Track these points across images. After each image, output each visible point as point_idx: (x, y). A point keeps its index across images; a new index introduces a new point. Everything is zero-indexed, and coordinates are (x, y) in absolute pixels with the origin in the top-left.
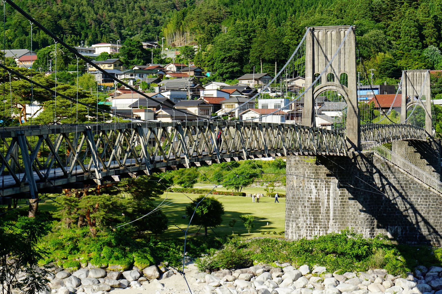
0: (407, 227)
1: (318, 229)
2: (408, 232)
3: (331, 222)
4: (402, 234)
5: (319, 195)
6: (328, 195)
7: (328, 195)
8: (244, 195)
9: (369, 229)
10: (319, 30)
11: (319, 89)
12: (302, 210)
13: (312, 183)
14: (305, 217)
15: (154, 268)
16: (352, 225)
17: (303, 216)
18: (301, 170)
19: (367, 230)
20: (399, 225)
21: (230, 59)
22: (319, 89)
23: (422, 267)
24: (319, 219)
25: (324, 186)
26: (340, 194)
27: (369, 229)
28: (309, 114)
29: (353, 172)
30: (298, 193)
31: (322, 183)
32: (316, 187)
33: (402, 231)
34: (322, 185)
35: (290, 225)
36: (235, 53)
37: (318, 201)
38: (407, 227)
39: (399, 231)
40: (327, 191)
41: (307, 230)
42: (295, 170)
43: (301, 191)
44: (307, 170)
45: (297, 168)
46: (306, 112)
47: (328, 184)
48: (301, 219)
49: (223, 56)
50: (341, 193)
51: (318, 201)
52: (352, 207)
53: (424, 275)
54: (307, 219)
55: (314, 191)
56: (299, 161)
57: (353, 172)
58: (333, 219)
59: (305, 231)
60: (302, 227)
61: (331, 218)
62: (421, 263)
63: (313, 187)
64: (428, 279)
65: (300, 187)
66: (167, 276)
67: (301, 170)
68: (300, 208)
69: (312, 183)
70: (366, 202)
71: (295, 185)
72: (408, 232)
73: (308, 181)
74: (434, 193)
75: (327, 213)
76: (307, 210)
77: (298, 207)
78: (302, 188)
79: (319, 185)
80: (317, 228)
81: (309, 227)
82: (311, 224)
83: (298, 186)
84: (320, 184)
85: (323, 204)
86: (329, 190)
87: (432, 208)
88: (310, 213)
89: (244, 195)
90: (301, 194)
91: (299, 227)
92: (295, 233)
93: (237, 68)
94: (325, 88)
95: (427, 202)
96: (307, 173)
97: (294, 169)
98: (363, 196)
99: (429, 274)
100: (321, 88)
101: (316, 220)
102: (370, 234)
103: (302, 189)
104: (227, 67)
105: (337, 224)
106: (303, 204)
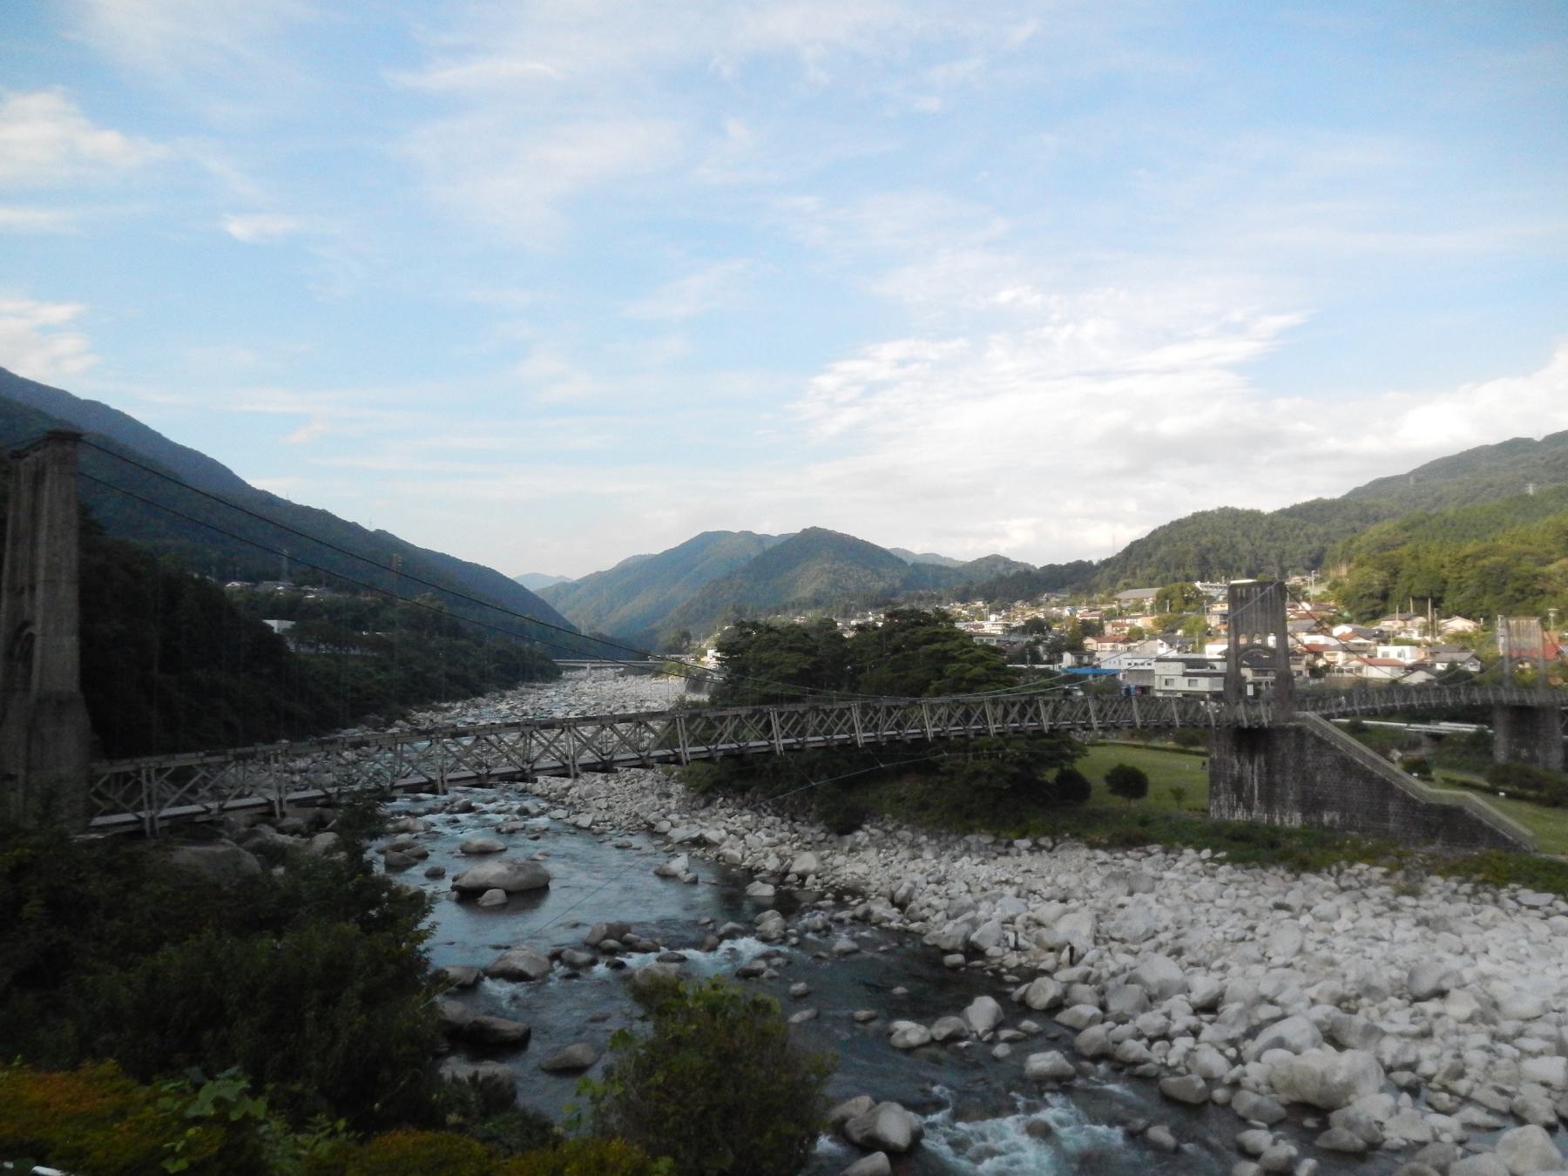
3: (1256, 803)
6: (1253, 772)
7: (1253, 772)
15: (1047, 838)
21: (1371, 596)
23: (1343, 863)
32: (1239, 761)
36: (1377, 587)
39: (1337, 818)
45: (1217, 740)
48: (1222, 797)
49: (1361, 593)
53: (1340, 872)
55: (1237, 766)
61: (1256, 797)
62: (1346, 858)
63: (1236, 762)
64: (1343, 877)
66: (1062, 849)
68: (1221, 785)
76: (1229, 788)
85: (1247, 779)
93: (1380, 607)
94: (1251, 650)
99: (1347, 871)
101: (1239, 799)
104: (1367, 605)
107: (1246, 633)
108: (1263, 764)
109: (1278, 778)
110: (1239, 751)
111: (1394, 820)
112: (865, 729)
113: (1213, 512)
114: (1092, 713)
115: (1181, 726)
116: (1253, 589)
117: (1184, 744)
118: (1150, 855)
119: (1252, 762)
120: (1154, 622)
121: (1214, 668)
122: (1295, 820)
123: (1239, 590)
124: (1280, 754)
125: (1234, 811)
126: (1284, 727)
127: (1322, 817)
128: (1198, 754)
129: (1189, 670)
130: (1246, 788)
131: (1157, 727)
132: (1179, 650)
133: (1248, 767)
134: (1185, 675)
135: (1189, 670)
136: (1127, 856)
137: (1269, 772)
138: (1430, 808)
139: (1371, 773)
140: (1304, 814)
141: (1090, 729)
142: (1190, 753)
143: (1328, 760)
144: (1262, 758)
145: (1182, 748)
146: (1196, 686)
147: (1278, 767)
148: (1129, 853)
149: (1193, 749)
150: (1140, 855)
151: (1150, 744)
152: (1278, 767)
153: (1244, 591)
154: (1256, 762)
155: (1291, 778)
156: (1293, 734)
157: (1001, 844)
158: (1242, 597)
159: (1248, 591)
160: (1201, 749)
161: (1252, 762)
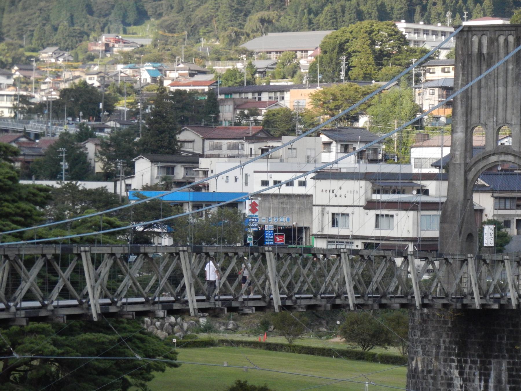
10: (482, 33)
11: (479, 161)
13: (454, 365)
18: (432, 336)
22: (479, 161)
25: (477, 373)
28: (454, 214)
30: (425, 386)
31: (474, 366)
32: (461, 374)
40: (482, 383)
42: (421, 335)
43: (431, 381)
44: (444, 336)
45: (424, 333)
46: (450, 209)
47: (486, 369)
55: (458, 382)
56: (428, 315)
63: (456, 373)
65: (429, 372)
67: (432, 336)
69: (454, 365)
71: (420, 369)
73: (445, 361)
78: (432, 374)
79: (467, 370)
83: (425, 369)
84: (470, 368)
86: (486, 381)
90: (431, 387)
94: (493, 159)
96: (444, 342)
97: (419, 333)
100: (484, 158)
103: (432, 378)
107: (485, 125)
108: (504, 377)
110: (462, 353)
114: (187, 280)
115: (357, 306)
116: (502, 39)
117: (365, 343)
119: (485, 376)
120: (315, 98)
121: (426, 192)
123: (475, 39)
128: (387, 360)
129: (377, 197)
131: (309, 307)
132: (360, 155)
133: (478, 383)
134: (370, 205)
135: (377, 197)
141: (183, 313)
142: (373, 359)
144: (504, 366)
145: (360, 349)
146: (390, 227)
149: (378, 350)
151: (298, 342)
153: (485, 41)
154: (493, 374)
159: (492, 42)
160: (394, 351)
161: (485, 376)
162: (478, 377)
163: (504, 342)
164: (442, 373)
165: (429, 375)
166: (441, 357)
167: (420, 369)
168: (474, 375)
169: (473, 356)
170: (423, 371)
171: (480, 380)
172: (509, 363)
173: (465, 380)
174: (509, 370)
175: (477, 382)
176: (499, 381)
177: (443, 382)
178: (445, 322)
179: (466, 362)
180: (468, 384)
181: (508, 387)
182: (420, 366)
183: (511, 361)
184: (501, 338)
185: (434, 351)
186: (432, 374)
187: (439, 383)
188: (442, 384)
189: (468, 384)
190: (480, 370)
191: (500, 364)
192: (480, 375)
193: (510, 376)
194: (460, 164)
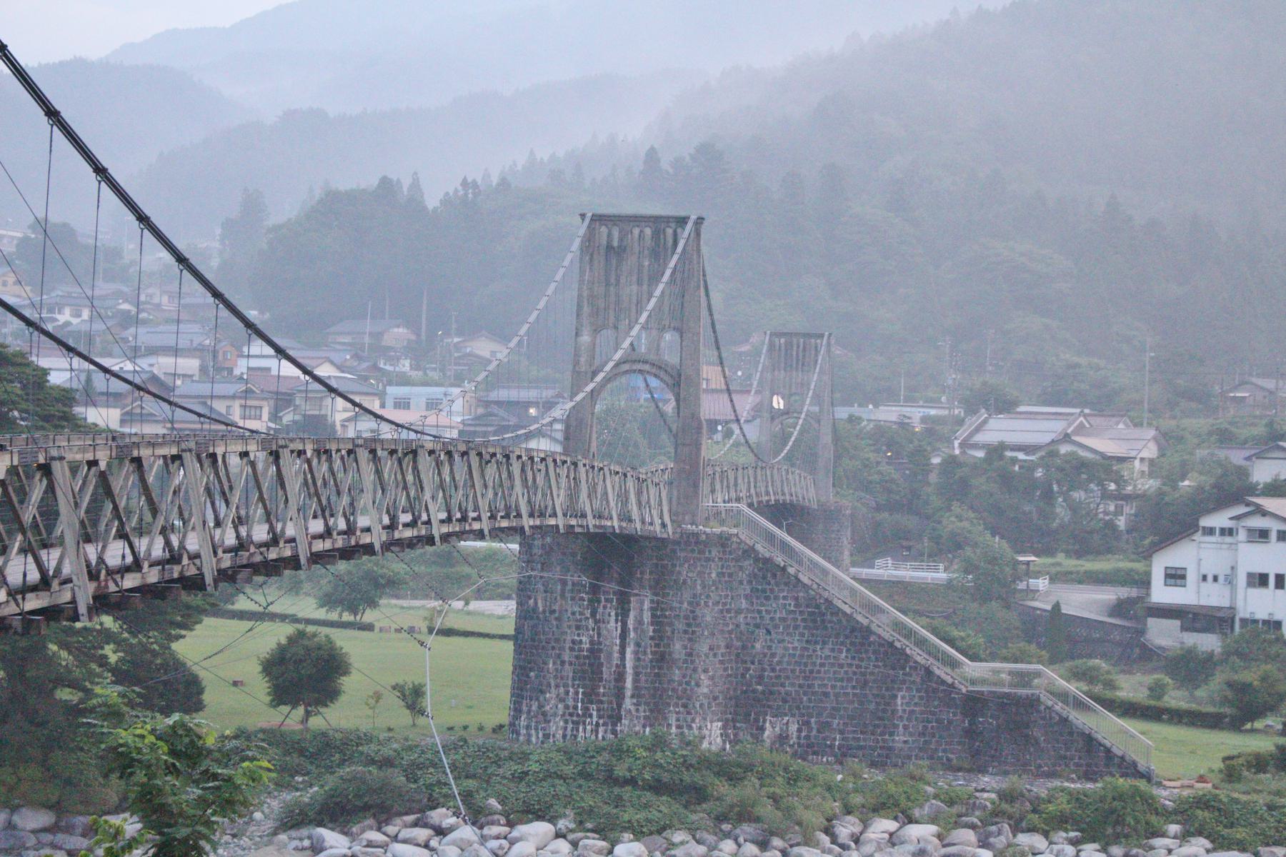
0: (813, 720)
1: (595, 719)
2: (814, 732)
3: (628, 703)
4: (799, 738)
5: (599, 635)
8: (369, 627)
9: (720, 724)
12: (556, 670)
14: (562, 690)
16: (677, 713)
17: (557, 686)
19: (715, 724)
20: (793, 716)
24: (598, 694)
25: (613, 614)
26: (651, 634)
27: (720, 724)
29: (685, 582)
31: (609, 605)
33: (799, 730)
34: (608, 610)
35: (525, 708)
37: (595, 651)
38: (813, 720)
39: (793, 728)
41: (566, 722)
43: (555, 623)
50: (654, 631)
51: (595, 651)
52: (679, 669)
54: (567, 693)
57: (685, 582)
58: (632, 696)
59: (562, 723)
60: (555, 715)
61: (628, 693)
70: (715, 655)
71: (541, 609)
72: (814, 732)
73: (573, 599)
74: (879, 636)
75: (616, 680)
77: (545, 663)
78: (557, 615)
79: (601, 610)
80: (591, 716)
81: (571, 715)
82: (576, 708)
84: (605, 607)
85: (609, 656)
87: (872, 673)
88: (574, 679)
89: (369, 627)
91: (544, 714)
92: (536, 729)
95: (861, 660)
98: (708, 641)
101: (591, 696)
102: (722, 735)
103: (556, 619)
105: (641, 708)
106: (559, 656)
108: (647, 617)
109: (678, 648)
111: (905, 727)
112: (531, 515)
113: (54, 64)
116: (636, 231)
118: (441, 832)
122: (712, 736)
124: (687, 596)
125: (576, 723)
126: (696, 535)
127: (762, 729)
130: (607, 673)
136: (395, 838)
137: (659, 637)
138: (974, 704)
139: (868, 631)
140: (724, 727)
143: (780, 606)
144: (646, 605)
147: (680, 625)
148: (391, 829)
150: (422, 834)
152: (680, 625)
154: (632, 615)
155: (705, 649)
156: (714, 552)
157: (69, 830)
158: (609, 247)
161: (623, 614)
162: (613, 618)
163: (647, 576)
164: (569, 612)
165: (553, 616)
166: (568, 595)
167: (541, 609)
168: (609, 615)
169: (608, 593)
170: (544, 611)
171: (617, 621)
172: (652, 601)
173: (596, 622)
174: (652, 609)
175: (612, 624)
176: (640, 622)
177: (570, 623)
178: (574, 554)
179: (599, 602)
180: (602, 625)
181: (651, 628)
182: (540, 604)
183: (655, 598)
184: (642, 573)
185: (559, 587)
186: (557, 615)
187: (565, 625)
188: (569, 627)
189: (602, 625)
190: (616, 609)
191: (642, 603)
192: (617, 615)
193: (653, 616)
194: (586, 373)
